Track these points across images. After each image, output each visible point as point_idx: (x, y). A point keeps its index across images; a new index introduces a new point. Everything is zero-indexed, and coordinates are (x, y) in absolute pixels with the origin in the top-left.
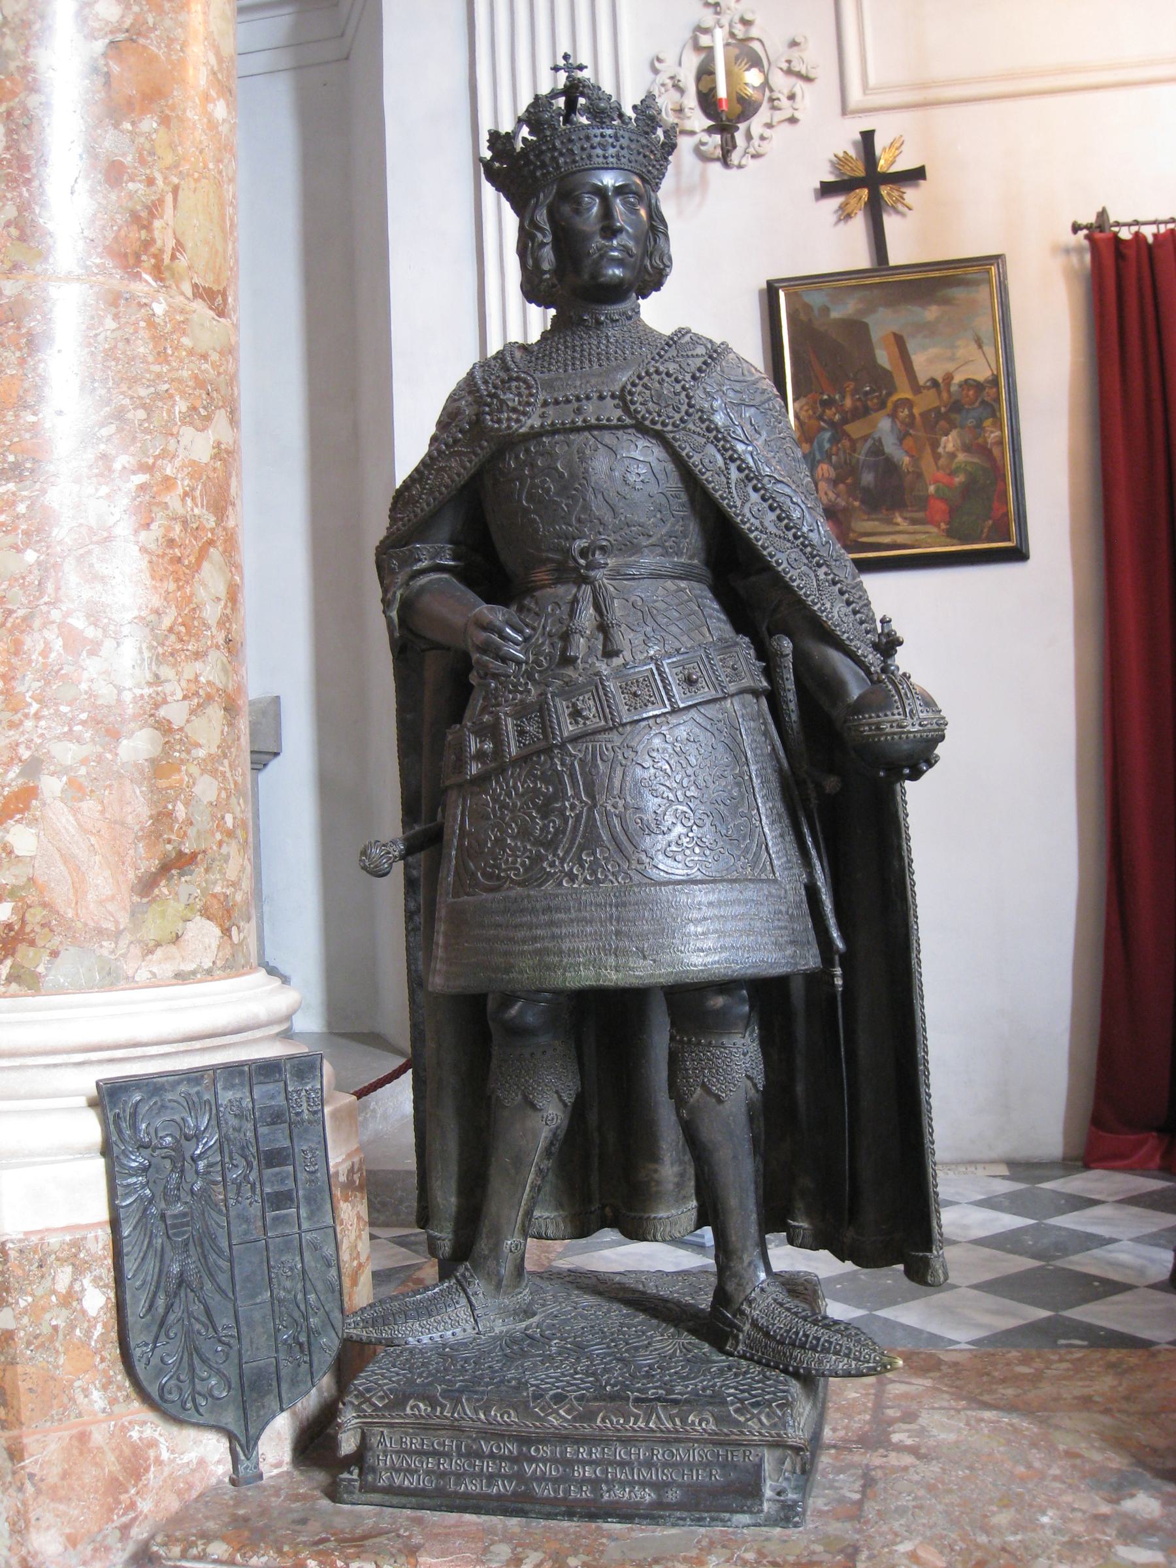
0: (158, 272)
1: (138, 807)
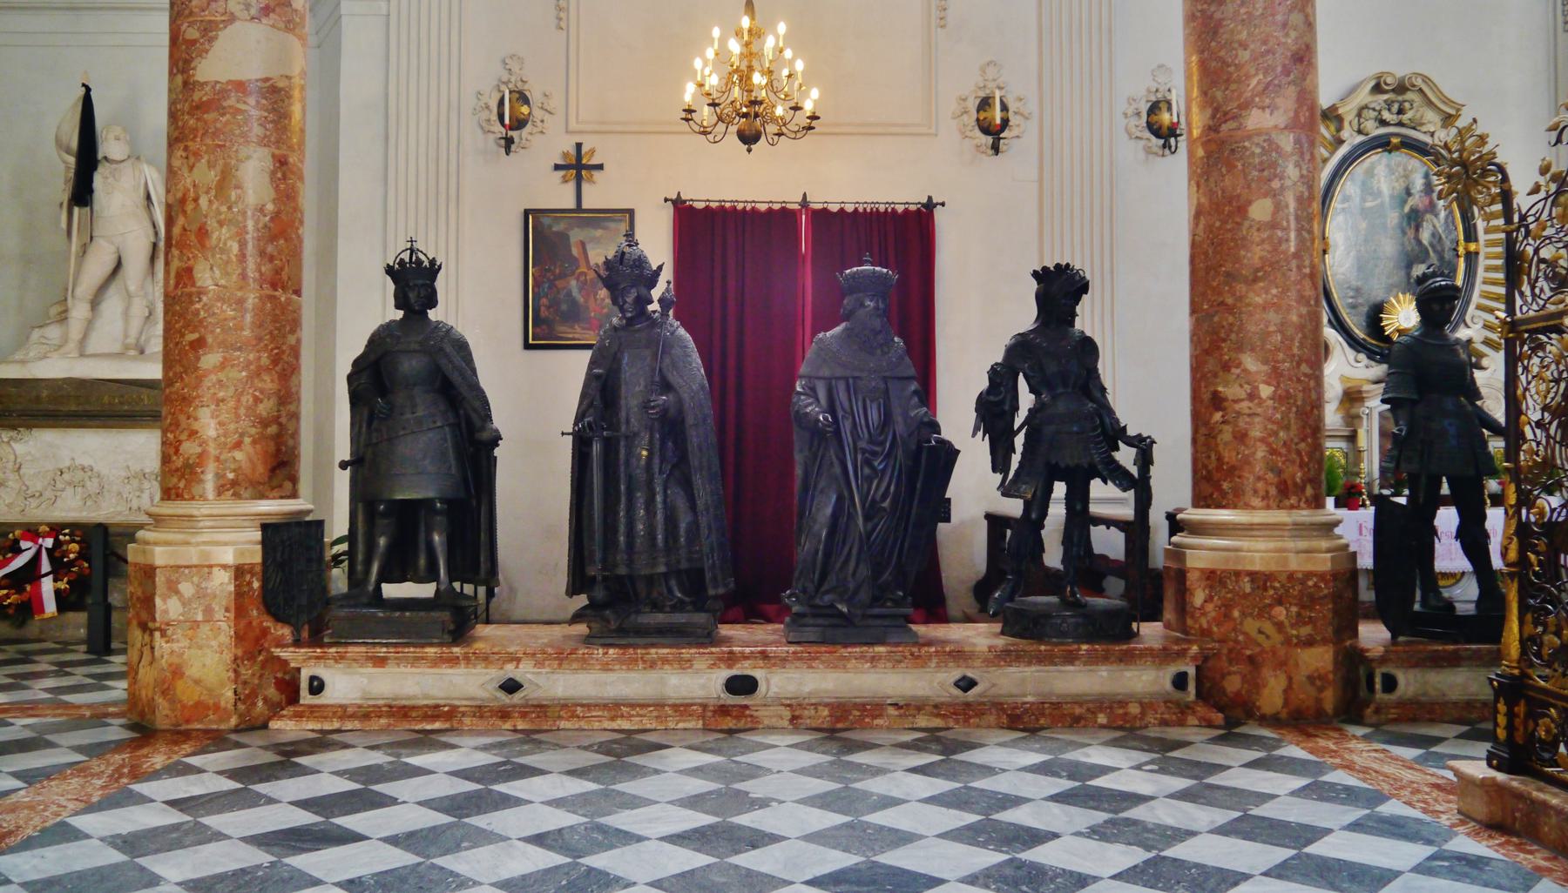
0: (283, 288)
1: (272, 448)
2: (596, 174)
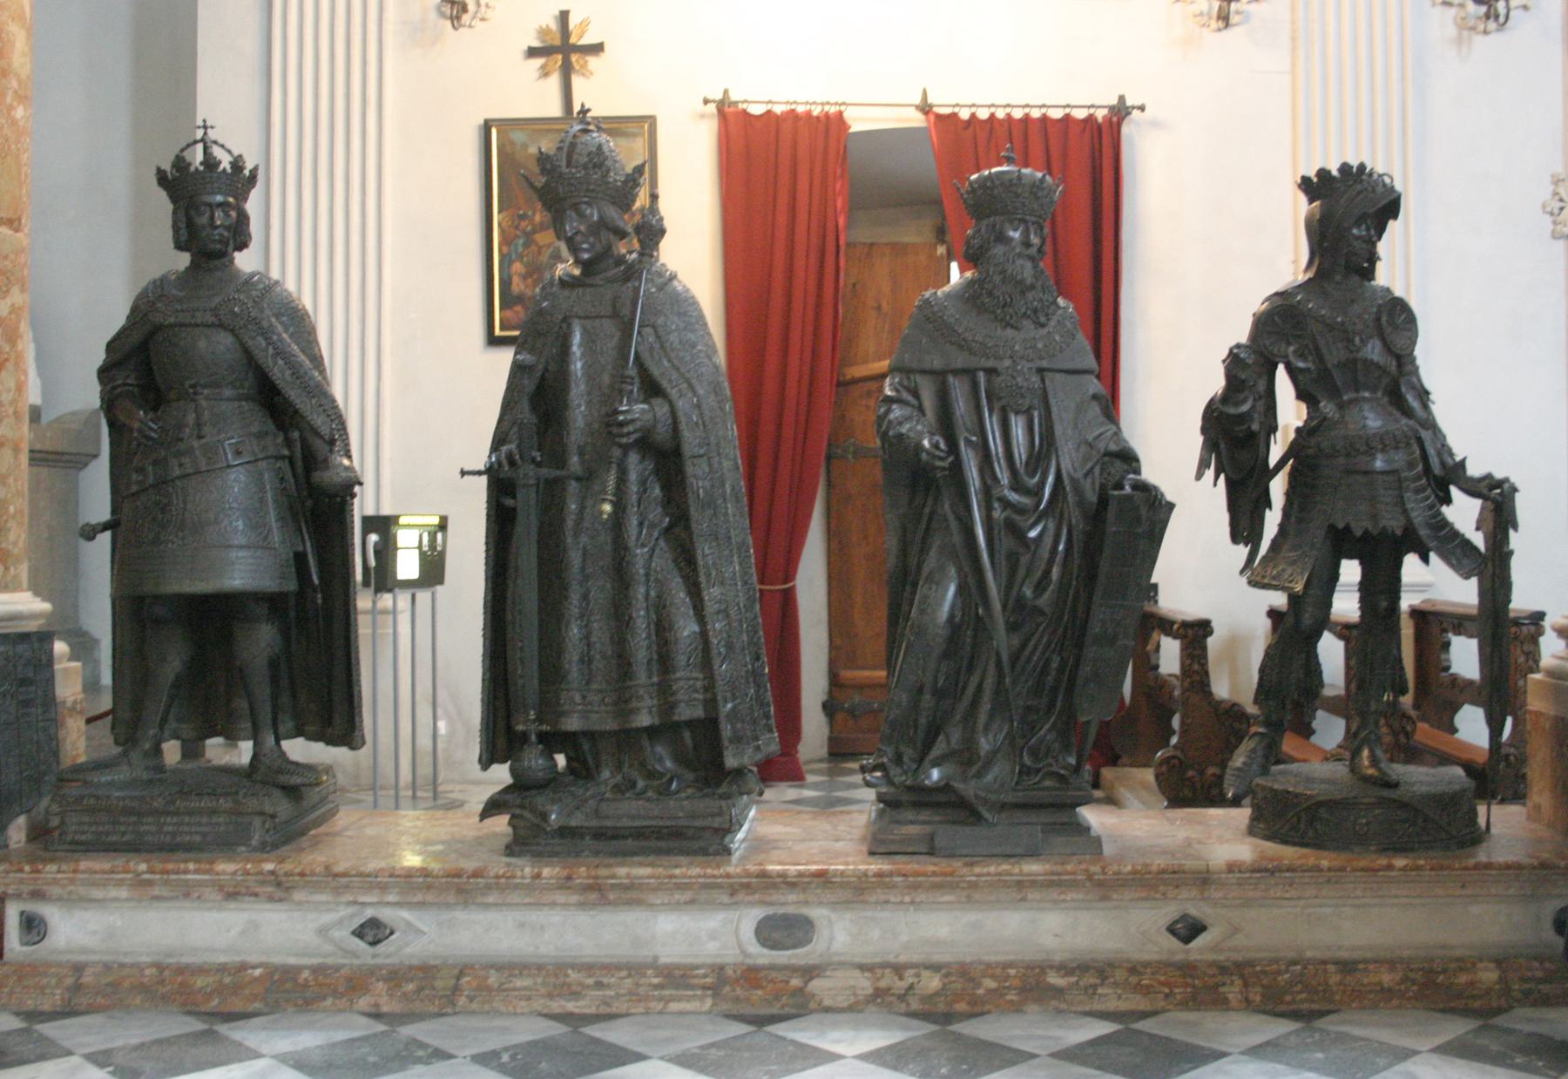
2: (593, 62)
